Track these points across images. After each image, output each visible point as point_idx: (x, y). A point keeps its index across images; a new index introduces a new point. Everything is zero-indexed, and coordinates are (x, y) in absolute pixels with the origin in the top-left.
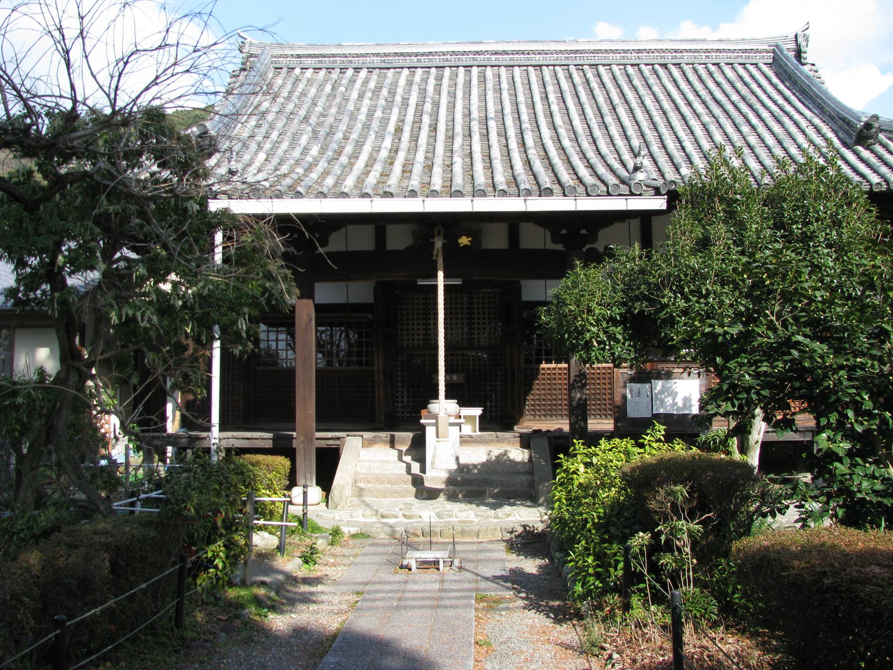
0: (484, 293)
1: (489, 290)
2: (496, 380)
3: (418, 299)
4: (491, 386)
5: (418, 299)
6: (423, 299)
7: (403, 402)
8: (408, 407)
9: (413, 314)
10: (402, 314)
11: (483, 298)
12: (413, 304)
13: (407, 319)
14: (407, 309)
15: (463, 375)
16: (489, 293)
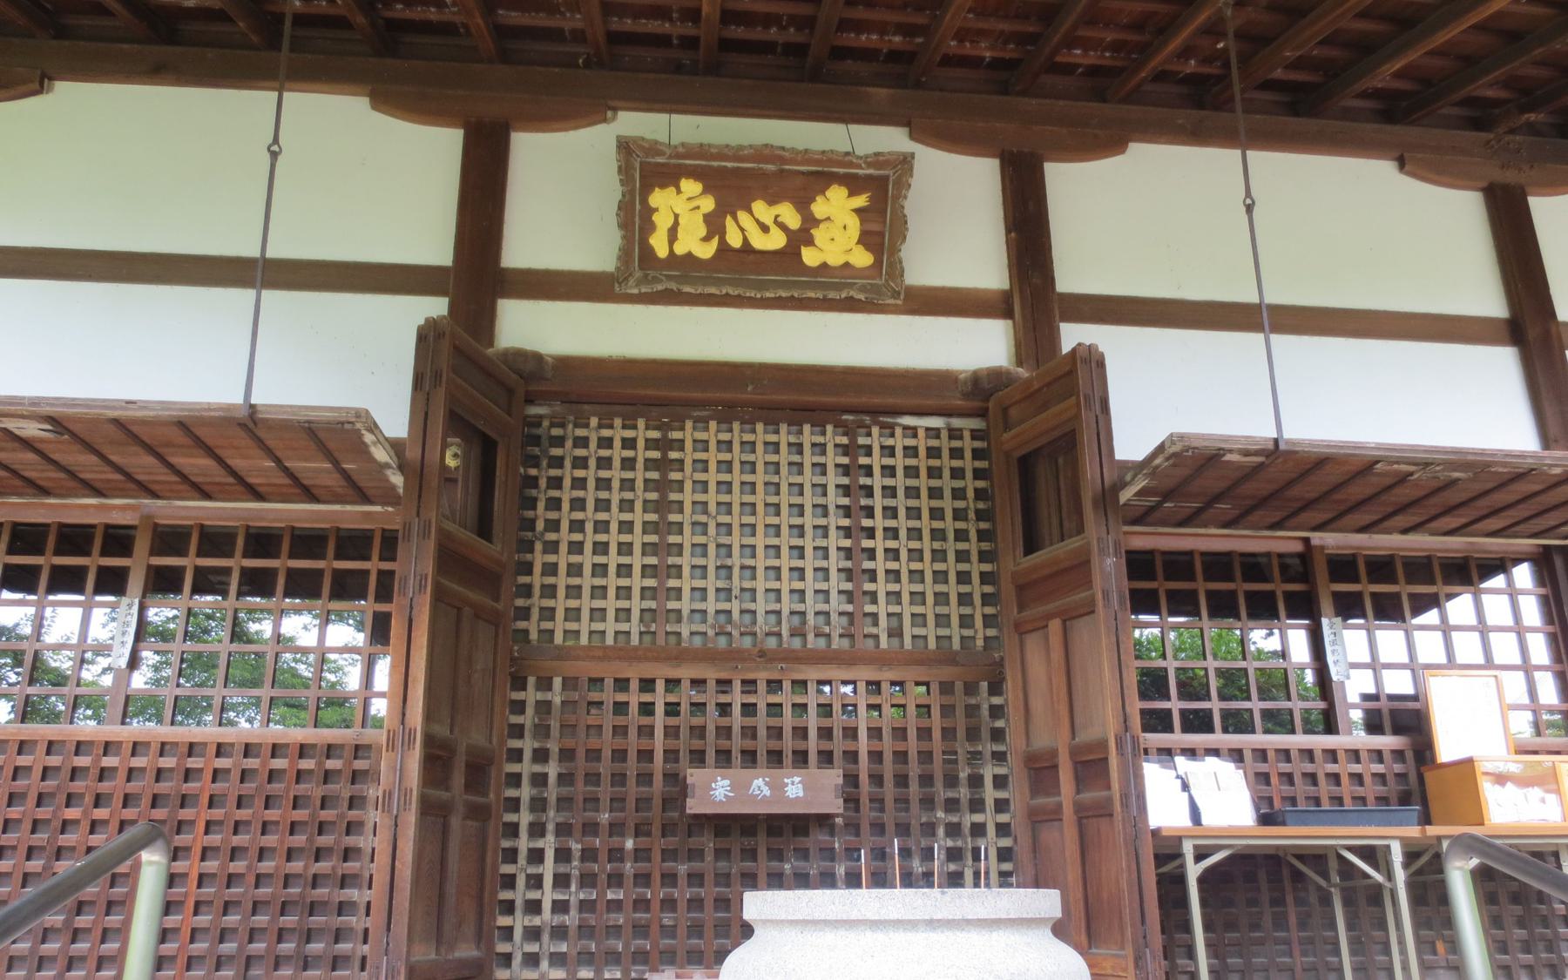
0: (913, 432)
1: (936, 422)
2: (977, 805)
3: (629, 444)
4: (953, 830)
5: (629, 444)
6: (651, 444)
7: (534, 907)
8: (560, 932)
9: (602, 505)
10: (555, 504)
11: (911, 451)
12: (604, 463)
13: (577, 526)
14: (580, 483)
15: (833, 777)
16: (933, 433)
